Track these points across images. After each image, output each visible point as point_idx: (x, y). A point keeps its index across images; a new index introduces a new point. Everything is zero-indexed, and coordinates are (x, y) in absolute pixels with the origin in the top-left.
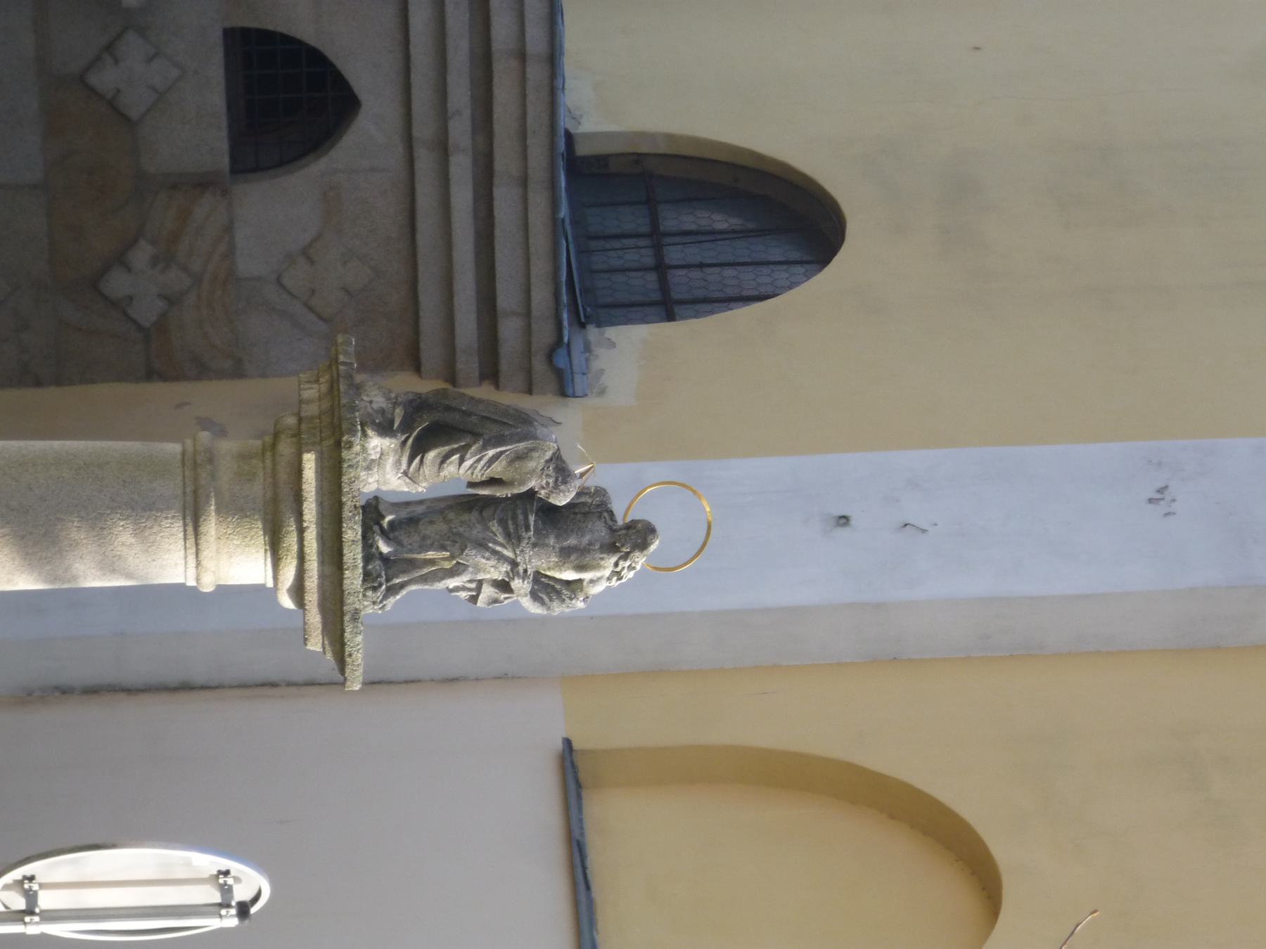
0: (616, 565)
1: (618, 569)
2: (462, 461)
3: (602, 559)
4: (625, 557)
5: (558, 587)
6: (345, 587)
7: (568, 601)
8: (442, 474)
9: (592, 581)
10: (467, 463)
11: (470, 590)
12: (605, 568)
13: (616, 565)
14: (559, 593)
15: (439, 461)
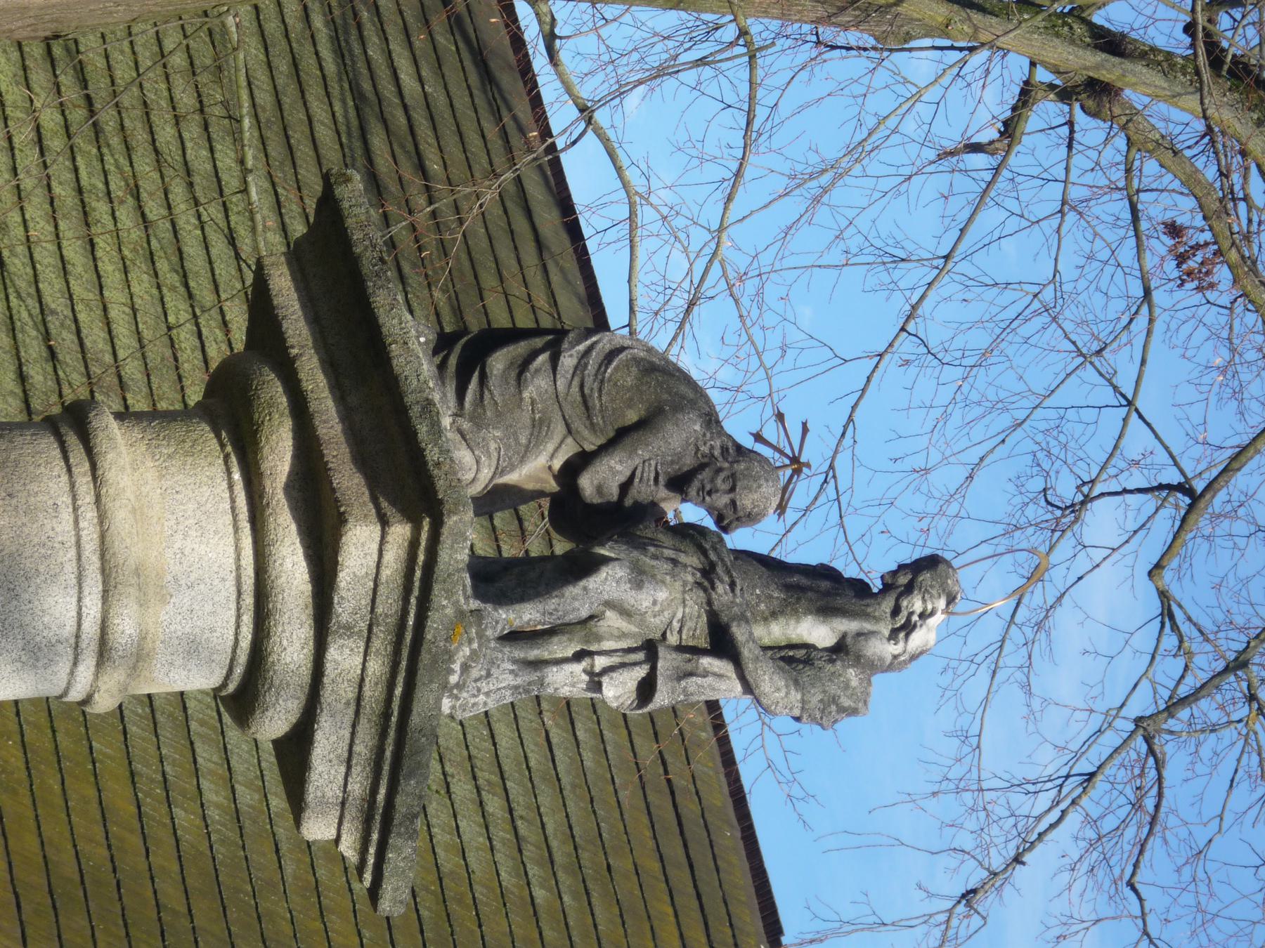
0: (896, 611)
1: (901, 620)
2: (554, 361)
3: (868, 605)
4: (909, 589)
5: (800, 653)
6: (397, 369)
7: (829, 667)
8: (526, 395)
9: (859, 634)
10: (568, 361)
11: (635, 664)
12: (877, 620)
13: (896, 611)
14: (808, 662)
15: (513, 374)
